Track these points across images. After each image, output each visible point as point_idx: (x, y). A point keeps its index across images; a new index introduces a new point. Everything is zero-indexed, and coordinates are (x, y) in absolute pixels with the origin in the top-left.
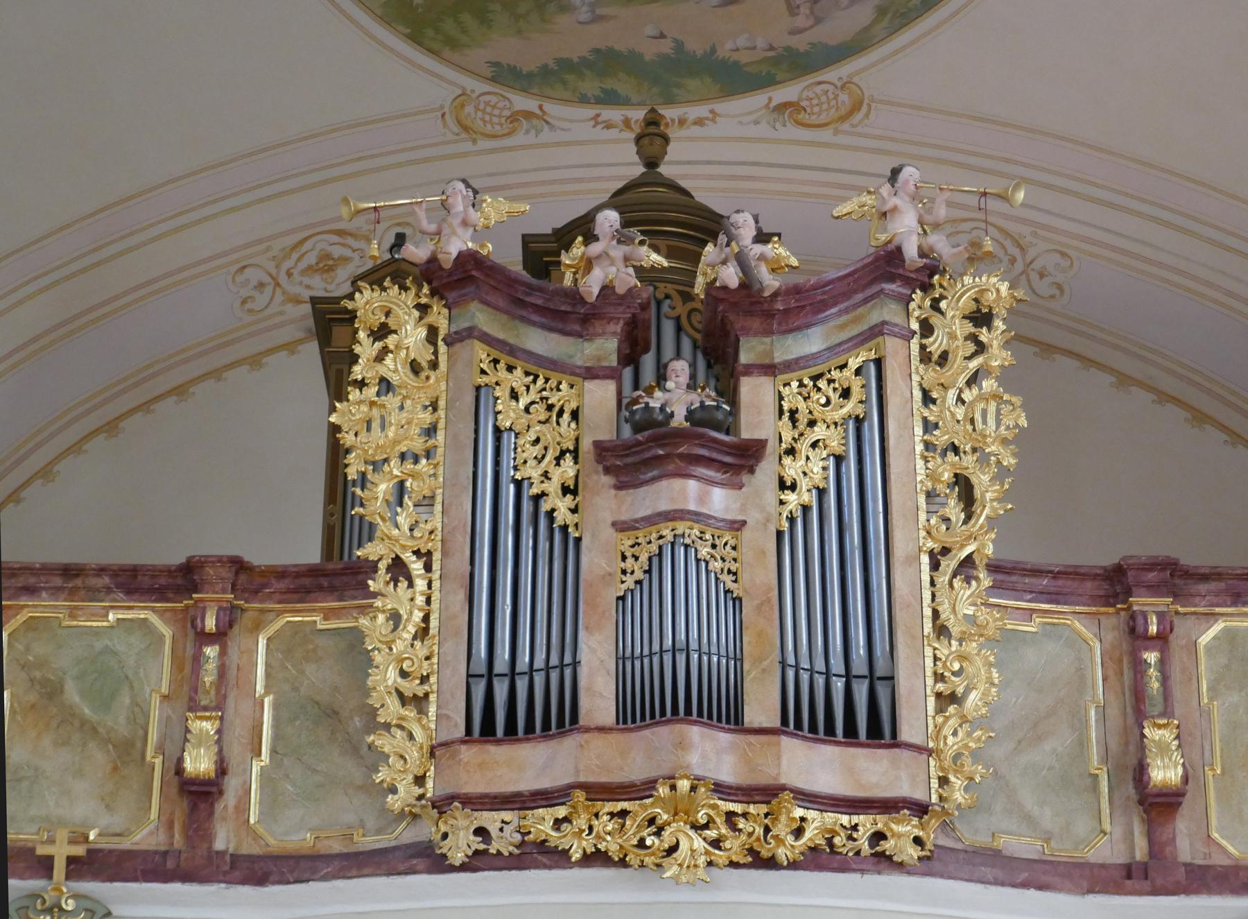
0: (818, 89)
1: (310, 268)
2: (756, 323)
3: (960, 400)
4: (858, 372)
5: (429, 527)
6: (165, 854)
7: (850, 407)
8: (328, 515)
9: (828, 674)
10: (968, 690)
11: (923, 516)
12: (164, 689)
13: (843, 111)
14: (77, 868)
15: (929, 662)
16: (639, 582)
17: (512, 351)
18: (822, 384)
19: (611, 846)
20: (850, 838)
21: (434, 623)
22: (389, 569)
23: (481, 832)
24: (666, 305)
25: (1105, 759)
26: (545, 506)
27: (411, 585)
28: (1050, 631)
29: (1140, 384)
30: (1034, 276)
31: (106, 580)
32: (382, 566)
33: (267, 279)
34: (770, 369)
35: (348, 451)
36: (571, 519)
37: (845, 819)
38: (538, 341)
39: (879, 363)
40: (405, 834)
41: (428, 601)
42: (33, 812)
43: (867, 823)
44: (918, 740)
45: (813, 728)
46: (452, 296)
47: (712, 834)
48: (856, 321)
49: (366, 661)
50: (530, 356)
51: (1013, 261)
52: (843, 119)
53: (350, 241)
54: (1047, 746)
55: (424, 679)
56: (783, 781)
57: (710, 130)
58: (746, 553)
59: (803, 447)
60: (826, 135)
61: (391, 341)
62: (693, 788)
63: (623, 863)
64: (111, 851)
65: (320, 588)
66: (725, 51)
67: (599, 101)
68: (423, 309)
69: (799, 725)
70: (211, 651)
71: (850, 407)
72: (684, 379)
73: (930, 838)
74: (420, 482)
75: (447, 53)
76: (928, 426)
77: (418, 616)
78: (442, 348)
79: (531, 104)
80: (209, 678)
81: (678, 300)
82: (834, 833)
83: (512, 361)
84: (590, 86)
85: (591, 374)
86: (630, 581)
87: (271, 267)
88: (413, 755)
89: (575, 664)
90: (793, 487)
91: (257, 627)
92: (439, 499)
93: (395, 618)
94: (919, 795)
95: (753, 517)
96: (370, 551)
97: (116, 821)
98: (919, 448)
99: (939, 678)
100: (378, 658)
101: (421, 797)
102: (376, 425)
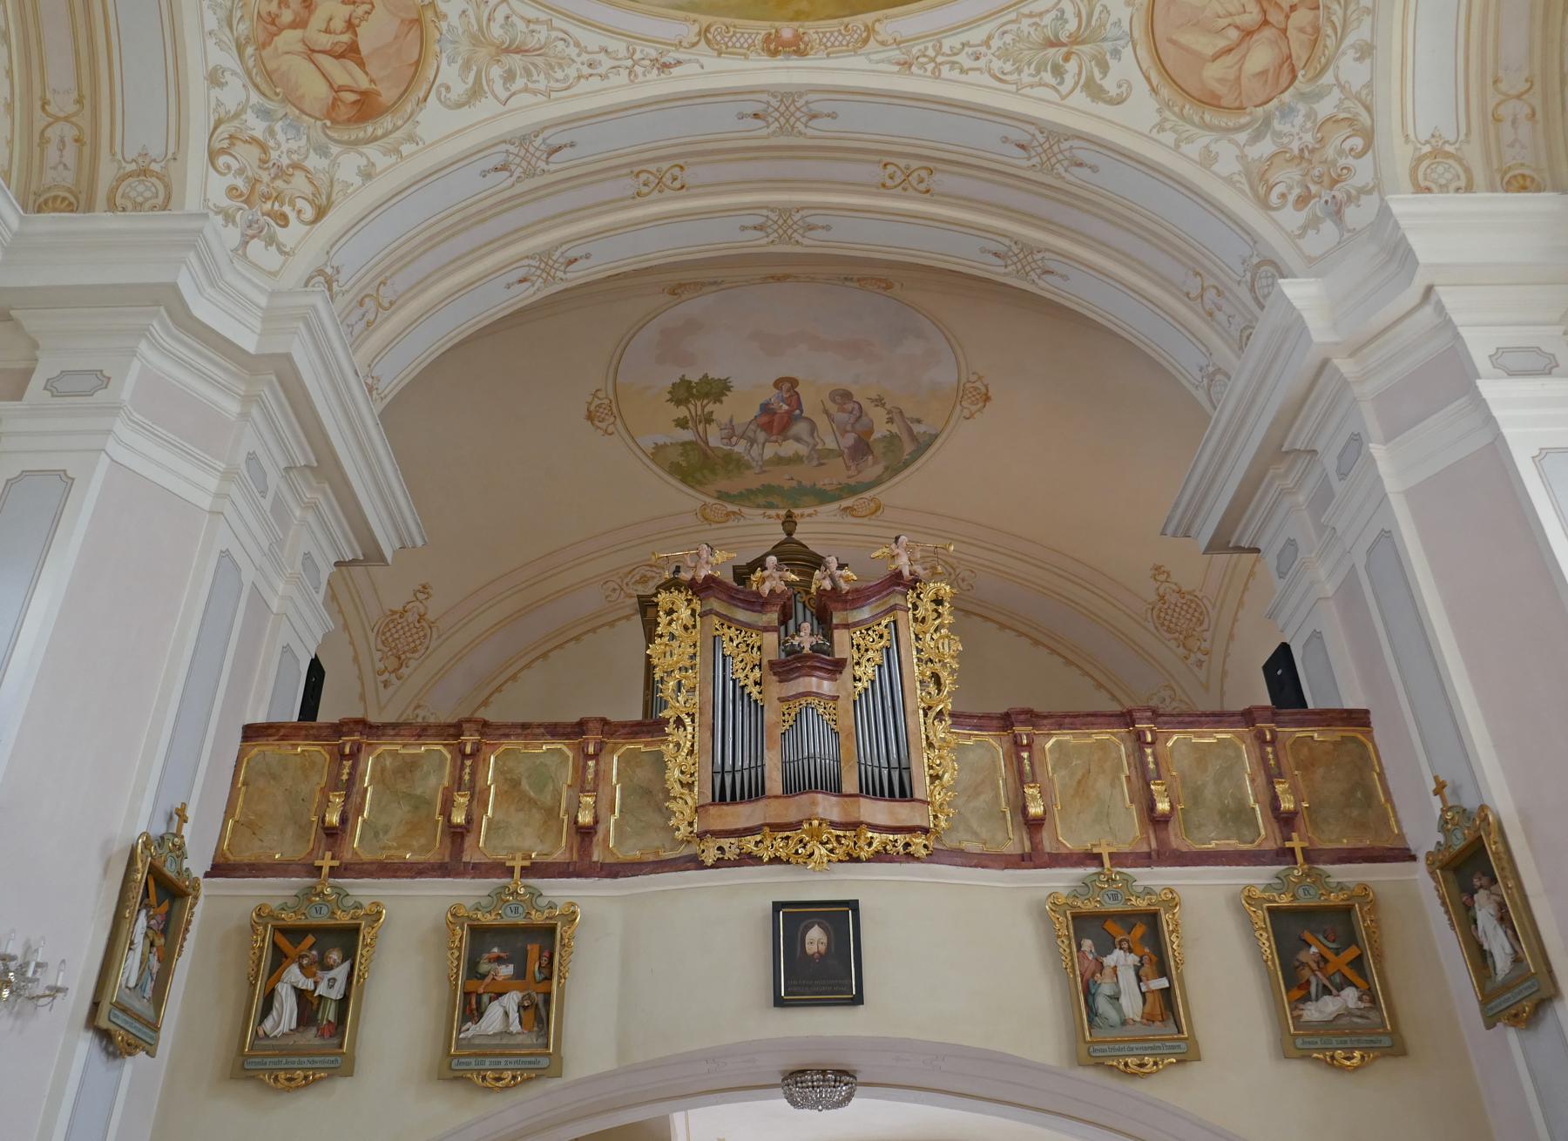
0: (861, 501)
1: (636, 582)
2: (840, 606)
3: (932, 638)
4: (886, 627)
5: (693, 702)
8: (645, 695)
10: (944, 773)
11: (919, 692)
12: (569, 782)
13: (873, 510)
14: (527, 872)
15: (926, 760)
16: (791, 726)
17: (730, 619)
18: (870, 632)
19: (782, 853)
20: (894, 846)
21: (696, 747)
22: (675, 722)
23: (720, 849)
24: (798, 597)
25: (1008, 804)
26: (747, 691)
27: (685, 730)
28: (979, 744)
29: (1010, 628)
30: (960, 581)
31: (542, 730)
32: (672, 721)
33: (617, 587)
34: (847, 626)
35: (655, 667)
36: (759, 697)
37: (891, 837)
38: (742, 615)
39: (895, 622)
40: (684, 851)
41: (693, 737)
42: (505, 844)
43: (901, 839)
44: (922, 798)
45: (874, 794)
46: (702, 595)
47: (829, 846)
48: (883, 604)
49: (665, 767)
51: (950, 574)
52: (873, 513)
53: (655, 569)
54: (982, 798)
55: (692, 775)
56: (862, 819)
57: (815, 518)
58: (840, 711)
59: (863, 661)
60: (865, 520)
61: (675, 616)
62: (820, 824)
63: (788, 862)
64: (542, 863)
65: (643, 732)
66: (819, 485)
67: (765, 507)
68: (689, 601)
69: (868, 792)
70: (591, 763)
72: (808, 631)
73: (931, 844)
74: (690, 680)
75: (697, 487)
76: (919, 651)
77: (689, 744)
78: (698, 619)
79: (735, 508)
80: (590, 776)
81: (804, 595)
82: (886, 844)
83: (729, 624)
84: (761, 500)
85: (766, 629)
86: (787, 725)
87: (619, 581)
88: (687, 811)
89: (763, 766)
90: (860, 680)
91: (613, 752)
92: (697, 689)
93: (678, 745)
94: (925, 824)
95: (842, 694)
96: (666, 714)
97: (546, 848)
98: (915, 661)
99: (931, 767)
101: (692, 832)
102: (668, 654)
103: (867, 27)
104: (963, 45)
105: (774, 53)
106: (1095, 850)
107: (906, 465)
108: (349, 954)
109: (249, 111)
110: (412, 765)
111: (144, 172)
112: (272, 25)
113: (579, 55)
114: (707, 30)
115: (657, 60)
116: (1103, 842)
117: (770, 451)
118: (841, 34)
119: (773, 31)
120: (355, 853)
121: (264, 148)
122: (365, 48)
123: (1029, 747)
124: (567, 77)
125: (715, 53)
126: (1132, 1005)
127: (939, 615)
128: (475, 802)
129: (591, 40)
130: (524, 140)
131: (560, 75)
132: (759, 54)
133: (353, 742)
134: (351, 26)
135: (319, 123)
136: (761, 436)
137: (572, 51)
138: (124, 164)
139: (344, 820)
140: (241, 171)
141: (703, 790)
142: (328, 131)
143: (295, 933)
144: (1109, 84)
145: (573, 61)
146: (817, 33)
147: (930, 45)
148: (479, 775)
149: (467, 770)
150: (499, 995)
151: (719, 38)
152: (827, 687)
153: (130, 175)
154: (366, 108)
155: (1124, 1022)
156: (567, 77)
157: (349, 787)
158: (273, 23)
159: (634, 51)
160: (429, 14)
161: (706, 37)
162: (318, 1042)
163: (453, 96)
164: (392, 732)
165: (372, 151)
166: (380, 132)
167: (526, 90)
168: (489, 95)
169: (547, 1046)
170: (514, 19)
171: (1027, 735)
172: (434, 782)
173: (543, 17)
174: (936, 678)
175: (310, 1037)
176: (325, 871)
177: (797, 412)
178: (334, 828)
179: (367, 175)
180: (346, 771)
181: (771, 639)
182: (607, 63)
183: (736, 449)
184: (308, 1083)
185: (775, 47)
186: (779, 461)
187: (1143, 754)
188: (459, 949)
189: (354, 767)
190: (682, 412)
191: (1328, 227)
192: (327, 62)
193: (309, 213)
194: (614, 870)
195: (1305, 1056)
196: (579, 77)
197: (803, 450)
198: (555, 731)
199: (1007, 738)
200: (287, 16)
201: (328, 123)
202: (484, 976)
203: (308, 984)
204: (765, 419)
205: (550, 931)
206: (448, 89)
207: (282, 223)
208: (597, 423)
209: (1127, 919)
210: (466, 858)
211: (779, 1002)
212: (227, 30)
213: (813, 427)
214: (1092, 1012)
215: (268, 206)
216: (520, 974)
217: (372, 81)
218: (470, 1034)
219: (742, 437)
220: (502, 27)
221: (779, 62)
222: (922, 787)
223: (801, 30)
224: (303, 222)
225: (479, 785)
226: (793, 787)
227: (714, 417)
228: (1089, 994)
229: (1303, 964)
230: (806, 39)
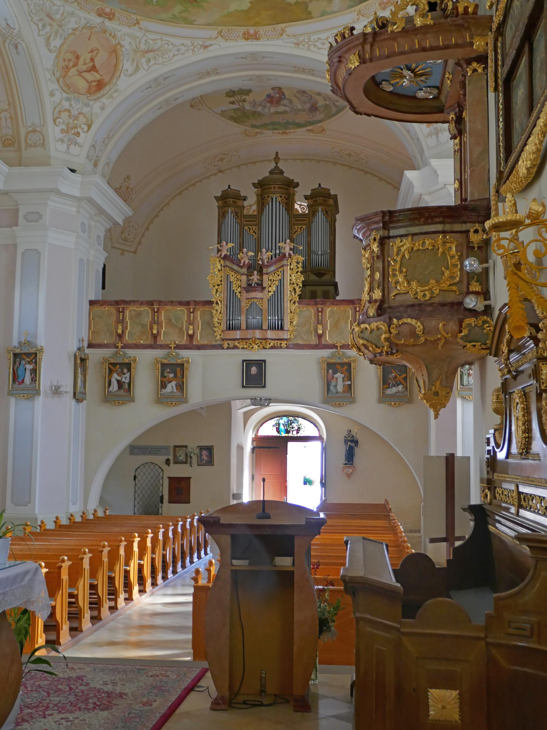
6: (187, 345)
7: (280, 277)
9: (275, 319)
12: (186, 320)
14: (175, 348)
19: (245, 346)
23: (228, 344)
24: (277, 198)
26: (237, 295)
32: (215, 302)
34: (267, 274)
38: (235, 267)
40: (218, 343)
43: (279, 342)
45: (273, 329)
47: (258, 345)
49: (213, 317)
50: (235, 270)
51: (357, 157)
60: (319, 135)
66: (297, 121)
68: (220, 261)
69: (271, 329)
70: (192, 314)
71: (280, 277)
73: (288, 343)
76: (290, 280)
77: (220, 310)
79: (260, 131)
80: (192, 319)
85: (243, 274)
86: (248, 307)
91: (198, 310)
93: (217, 310)
98: (289, 283)
99: (290, 319)
100: (215, 316)
103: (282, 29)
104: (319, 39)
105: (247, 39)
106: (336, 345)
107: (334, 115)
108: (129, 370)
109: (63, 100)
110: (139, 314)
111: (34, 131)
112: (67, 69)
113: (173, 48)
114: (221, 32)
115: (203, 45)
116: (339, 343)
117: (273, 110)
118: (272, 31)
119: (246, 30)
120: (127, 341)
121: (69, 111)
122: (97, 66)
123: (321, 312)
124: (169, 56)
125: (225, 40)
126: (340, 388)
127: (298, 268)
128: (159, 327)
129: (177, 41)
130: (155, 79)
131: (166, 56)
132: (241, 40)
133: (122, 307)
134: (92, 60)
135: (85, 96)
136: (268, 105)
137: (171, 47)
138: (28, 128)
139: (123, 331)
140: (63, 122)
141: (223, 326)
142: (89, 98)
143: (114, 365)
145: (171, 50)
146: (263, 31)
147: (306, 37)
148: (160, 317)
149: (156, 316)
150: (170, 382)
151: (226, 34)
152: (258, 295)
153: (30, 132)
154: (100, 85)
155: (337, 393)
156: (169, 56)
157: (122, 322)
158: (67, 68)
159: (194, 43)
160: (118, 47)
161: (220, 34)
162: (124, 393)
163: (129, 72)
164: (133, 303)
165: (104, 100)
166: (105, 92)
167: (155, 64)
168: (142, 69)
169: (184, 396)
170: (149, 41)
171: (321, 308)
172: (147, 319)
173: (159, 37)
174: (294, 289)
175: (122, 392)
176: (120, 347)
177: (283, 97)
178: (120, 335)
179: (103, 108)
180: (121, 316)
181: (244, 278)
182: (183, 49)
183: (258, 110)
184: (123, 404)
185: (247, 37)
186: (277, 113)
187: (356, 314)
188: (159, 370)
189: (123, 315)
190: (232, 99)
191: (434, 137)
192: (84, 74)
193: (86, 128)
194: (199, 347)
195: (383, 402)
196: (174, 56)
197: (288, 109)
198: (181, 303)
199: (315, 307)
200: (71, 64)
201: (88, 95)
202: (166, 377)
203: (119, 378)
204: (269, 99)
205: (183, 365)
206: (127, 70)
207: (78, 135)
208: (194, 107)
209: (342, 364)
210: (158, 343)
211: (243, 387)
212: (53, 77)
213: (291, 102)
214: (328, 390)
215: (73, 132)
216: (175, 376)
217: (101, 76)
218: (163, 392)
219: (260, 105)
220: (144, 44)
221: (249, 42)
222: (287, 326)
223: (257, 30)
224: (85, 132)
225: (160, 320)
226: (248, 328)
227: (246, 100)
228: (328, 385)
229: (390, 378)
230: (259, 33)
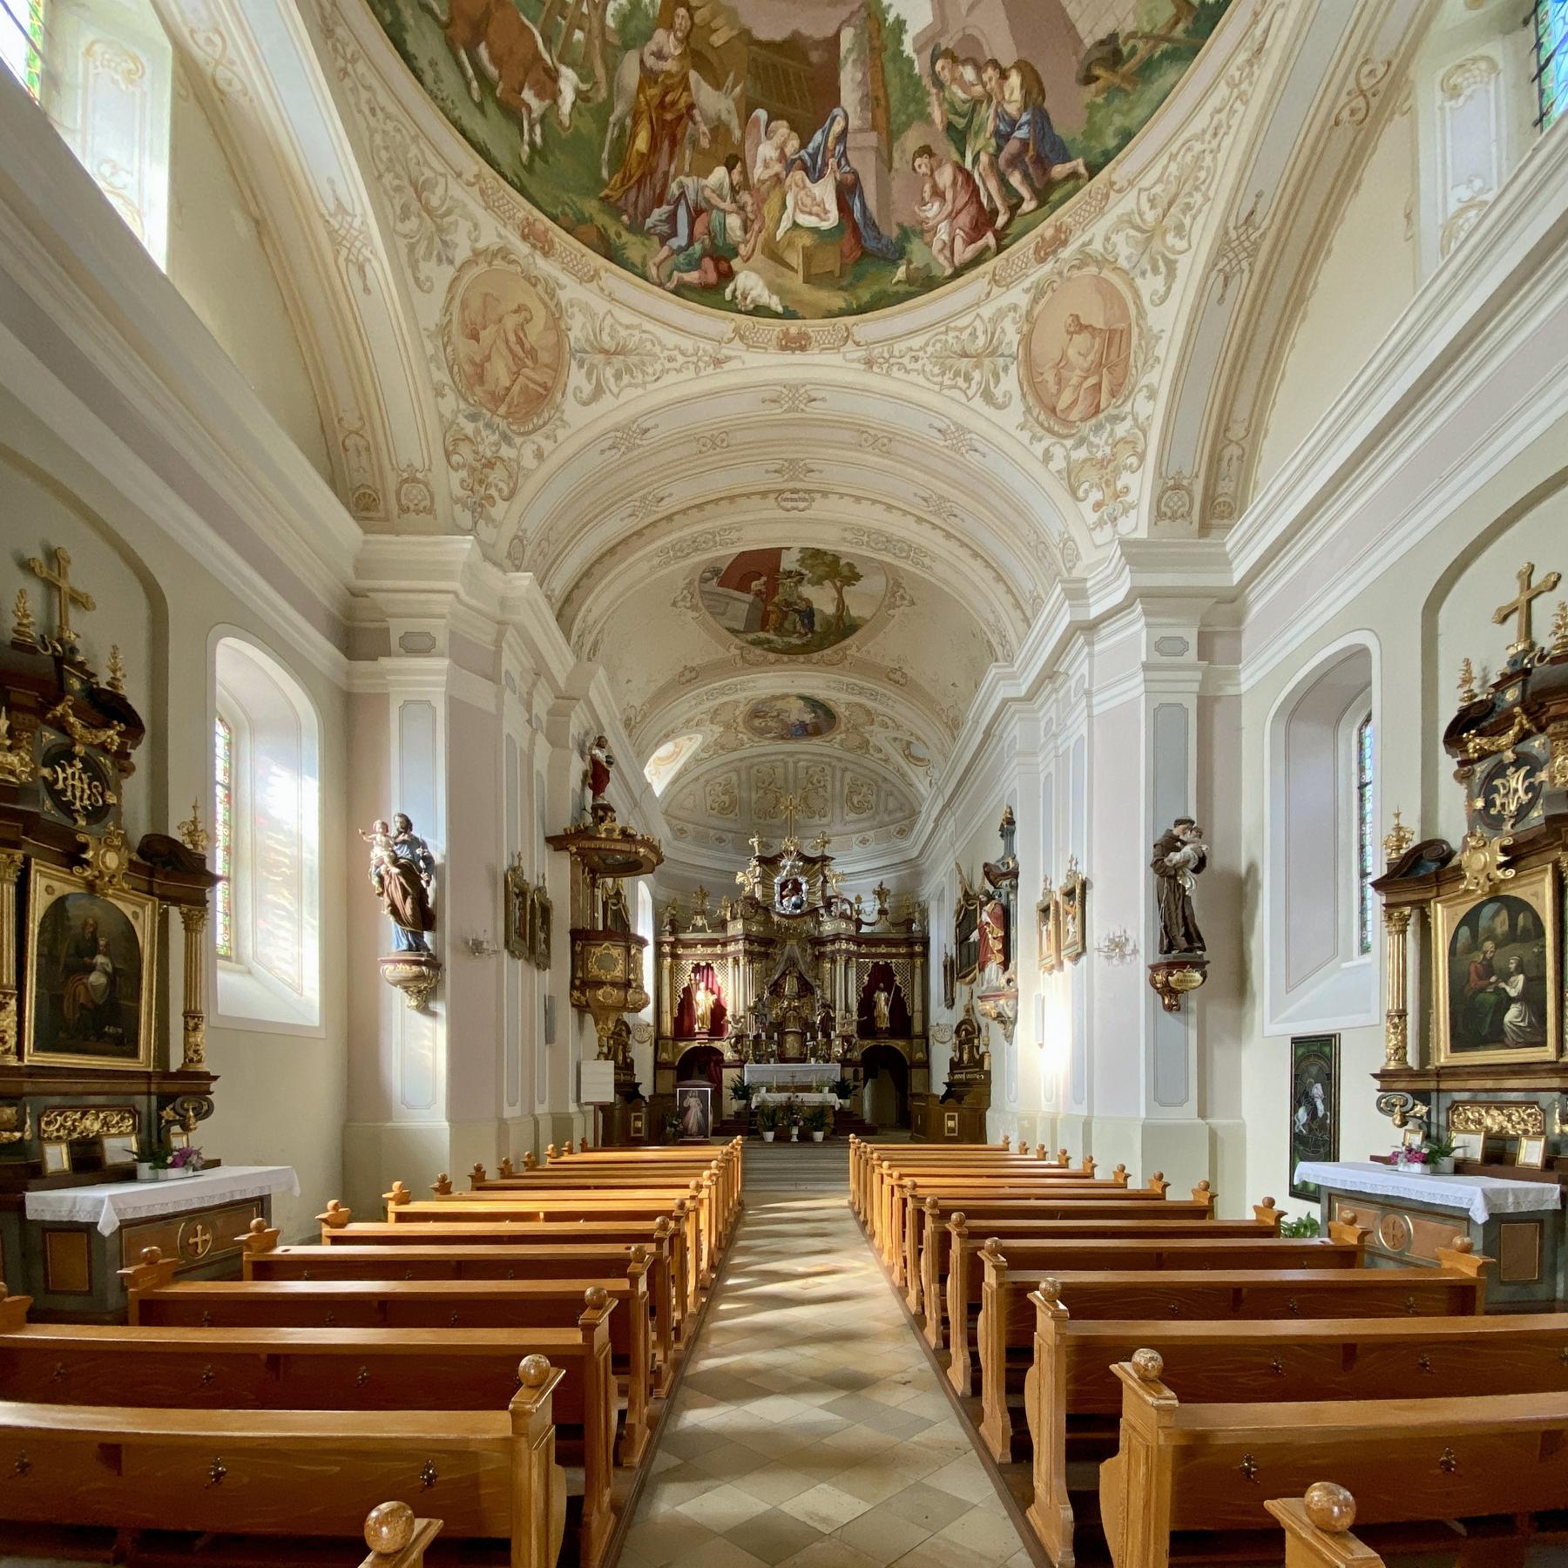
144: (998, 392)
165: (538, 437)
166: (541, 422)
167: (630, 385)
